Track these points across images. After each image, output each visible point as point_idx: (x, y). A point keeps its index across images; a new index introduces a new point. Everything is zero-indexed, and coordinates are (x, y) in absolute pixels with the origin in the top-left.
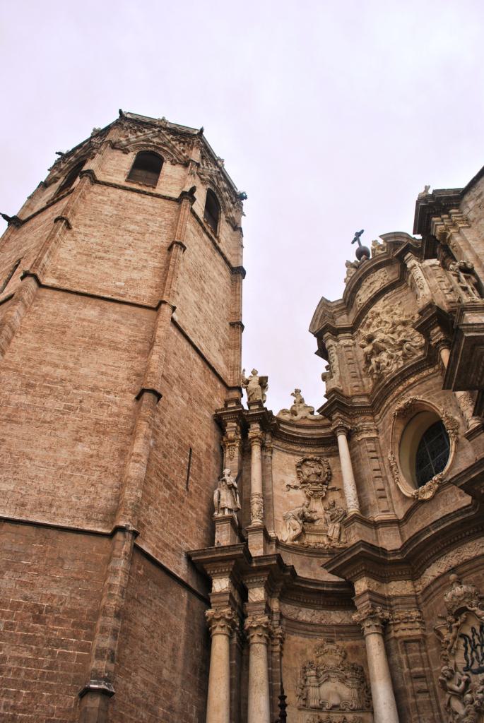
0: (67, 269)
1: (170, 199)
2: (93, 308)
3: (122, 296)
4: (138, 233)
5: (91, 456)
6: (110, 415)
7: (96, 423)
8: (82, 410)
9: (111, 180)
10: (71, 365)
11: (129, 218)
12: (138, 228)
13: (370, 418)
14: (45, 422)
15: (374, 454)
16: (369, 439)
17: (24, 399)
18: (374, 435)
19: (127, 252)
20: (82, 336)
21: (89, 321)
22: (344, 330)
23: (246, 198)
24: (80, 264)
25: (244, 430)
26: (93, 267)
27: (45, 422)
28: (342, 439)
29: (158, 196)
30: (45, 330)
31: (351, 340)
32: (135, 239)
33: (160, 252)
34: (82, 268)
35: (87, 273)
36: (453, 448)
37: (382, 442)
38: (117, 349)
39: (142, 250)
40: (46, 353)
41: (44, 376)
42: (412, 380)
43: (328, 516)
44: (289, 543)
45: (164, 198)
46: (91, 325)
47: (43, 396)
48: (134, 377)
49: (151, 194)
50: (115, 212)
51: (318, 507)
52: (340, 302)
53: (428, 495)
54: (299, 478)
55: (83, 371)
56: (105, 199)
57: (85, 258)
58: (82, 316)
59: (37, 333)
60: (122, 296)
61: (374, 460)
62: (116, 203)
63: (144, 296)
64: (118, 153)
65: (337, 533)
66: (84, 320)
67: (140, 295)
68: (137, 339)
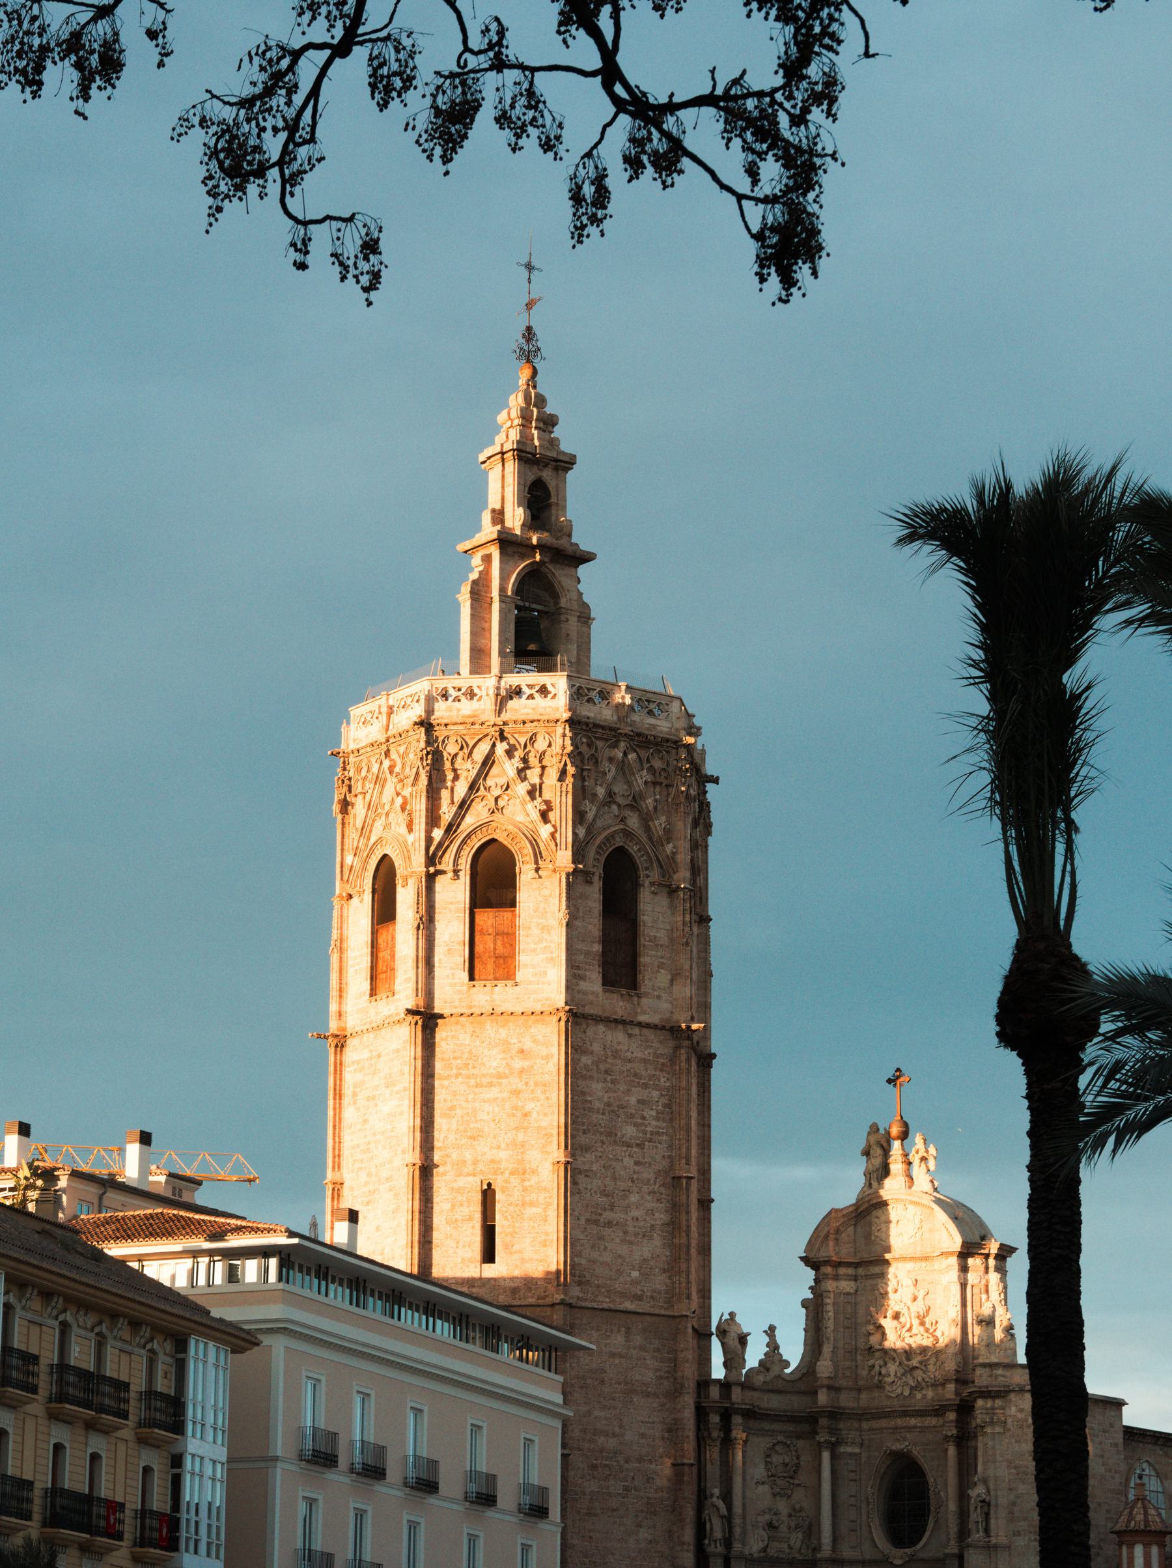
0: (583, 1261)
1: (663, 1028)
2: (619, 1331)
3: (639, 1298)
4: (638, 1145)
5: (651, 1542)
6: (656, 1491)
7: (648, 1503)
8: (636, 1489)
9: (585, 993)
10: (617, 1430)
11: (621, 1107)
12: (634, 1129)
13: (856, 1425)
14: (614, 1510)
15: (853, 1476)
16: (851, 1454)
17: (592, 1486)
18: (857, 1450)
19: (634, 1198)
20: (619, 1383)
21: (621, 1356)
22: (849, 1265)
23: (715, 780)
24: (593, 1247)
25: (726, 1427)
26: (606, 1248)
27: (614, 1510)
28: (826, 1455)
29: (648, 1026)
30: (589, 1381)
31: (852, 1283)
32: (637, 1163)
33: (663, 1185)
34: (595, 1254)
35: (602, 1263)
36: (930, 1526)
37: (863, 1460)
38: (648, 1395)
39: (645, 1188)
40: (596, 1418)
41: (601, 1451)
42: (913, 1421)
43: (793, 1524)
44: (756, 1555)
45: (655, 1027)
46: (623, 1361)
47: (606, 1478)
48: (666, 1435)
49: (640, 1024)
50: (605, 1099)
51: (782, 1506)
52: (851, 1209)
53: (898, 1562)
54: (768, 1470)
55: (628, 1436)
56: (589, 1062)
57: (594, 1229)
58: (612, 1350)
59: (582, 1388)
60: (639, 1298)
61: (852, 1483)
62: (602, 1067)
63: (660, 1292)
64: (581, 888)
65: (799, 1543)
66: (613, 1355)
67: (654, 1291)
68: (662, 1374)
